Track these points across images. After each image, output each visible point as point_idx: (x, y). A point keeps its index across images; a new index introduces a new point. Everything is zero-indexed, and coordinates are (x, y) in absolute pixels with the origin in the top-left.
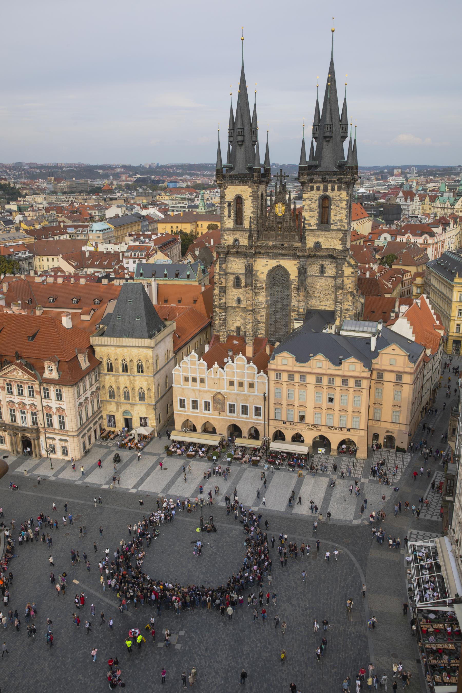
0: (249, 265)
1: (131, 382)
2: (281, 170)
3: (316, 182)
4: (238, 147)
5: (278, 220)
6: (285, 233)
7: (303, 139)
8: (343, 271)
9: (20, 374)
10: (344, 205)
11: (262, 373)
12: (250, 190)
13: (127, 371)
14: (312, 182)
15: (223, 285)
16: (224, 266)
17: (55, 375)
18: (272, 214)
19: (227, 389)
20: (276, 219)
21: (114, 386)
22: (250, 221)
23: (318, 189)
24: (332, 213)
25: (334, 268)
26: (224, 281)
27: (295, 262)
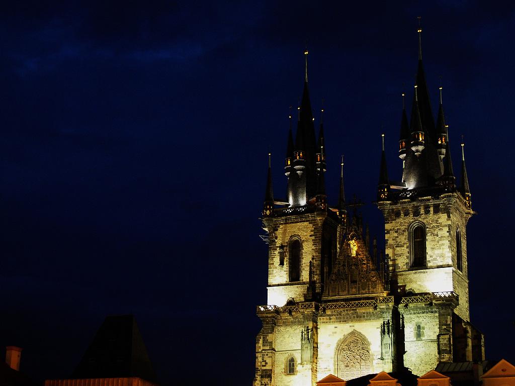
15: (268, 367)
22: (310, 269)
23: (407, 214)
26: (269, 360)
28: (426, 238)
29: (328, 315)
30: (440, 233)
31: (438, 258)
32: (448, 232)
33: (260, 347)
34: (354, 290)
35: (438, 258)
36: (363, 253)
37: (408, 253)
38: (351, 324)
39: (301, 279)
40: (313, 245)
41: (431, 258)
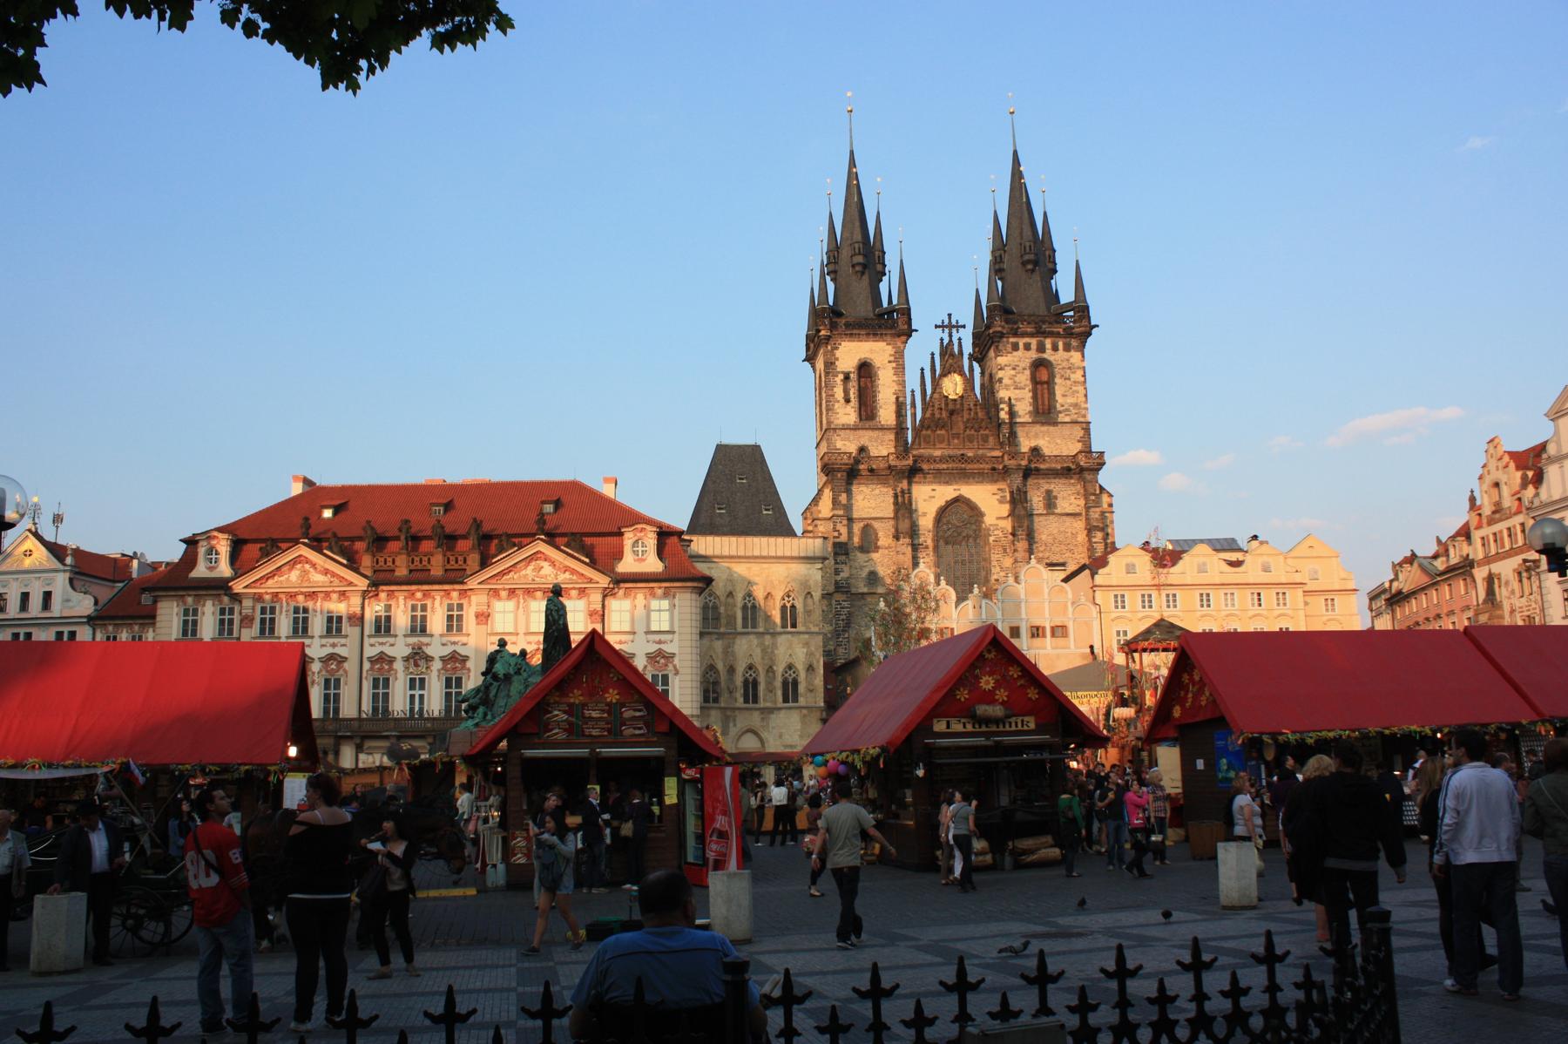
0: (903, 492)
1: (764, 651)
3: (1024, 335)
5: (951, 407)
8: (1098, 496)
9: (547, 569)
10: (1078, 376)
11: (1083, 600)
12: (889, 350)
13: (754, 626)
14: (1016, 335)
15: (844, 538)
16: (843, 498)
17: (653, 564)
21: (720, 666)
23: (1027, 347)
27: (993, 488)
30: (1073, 377)
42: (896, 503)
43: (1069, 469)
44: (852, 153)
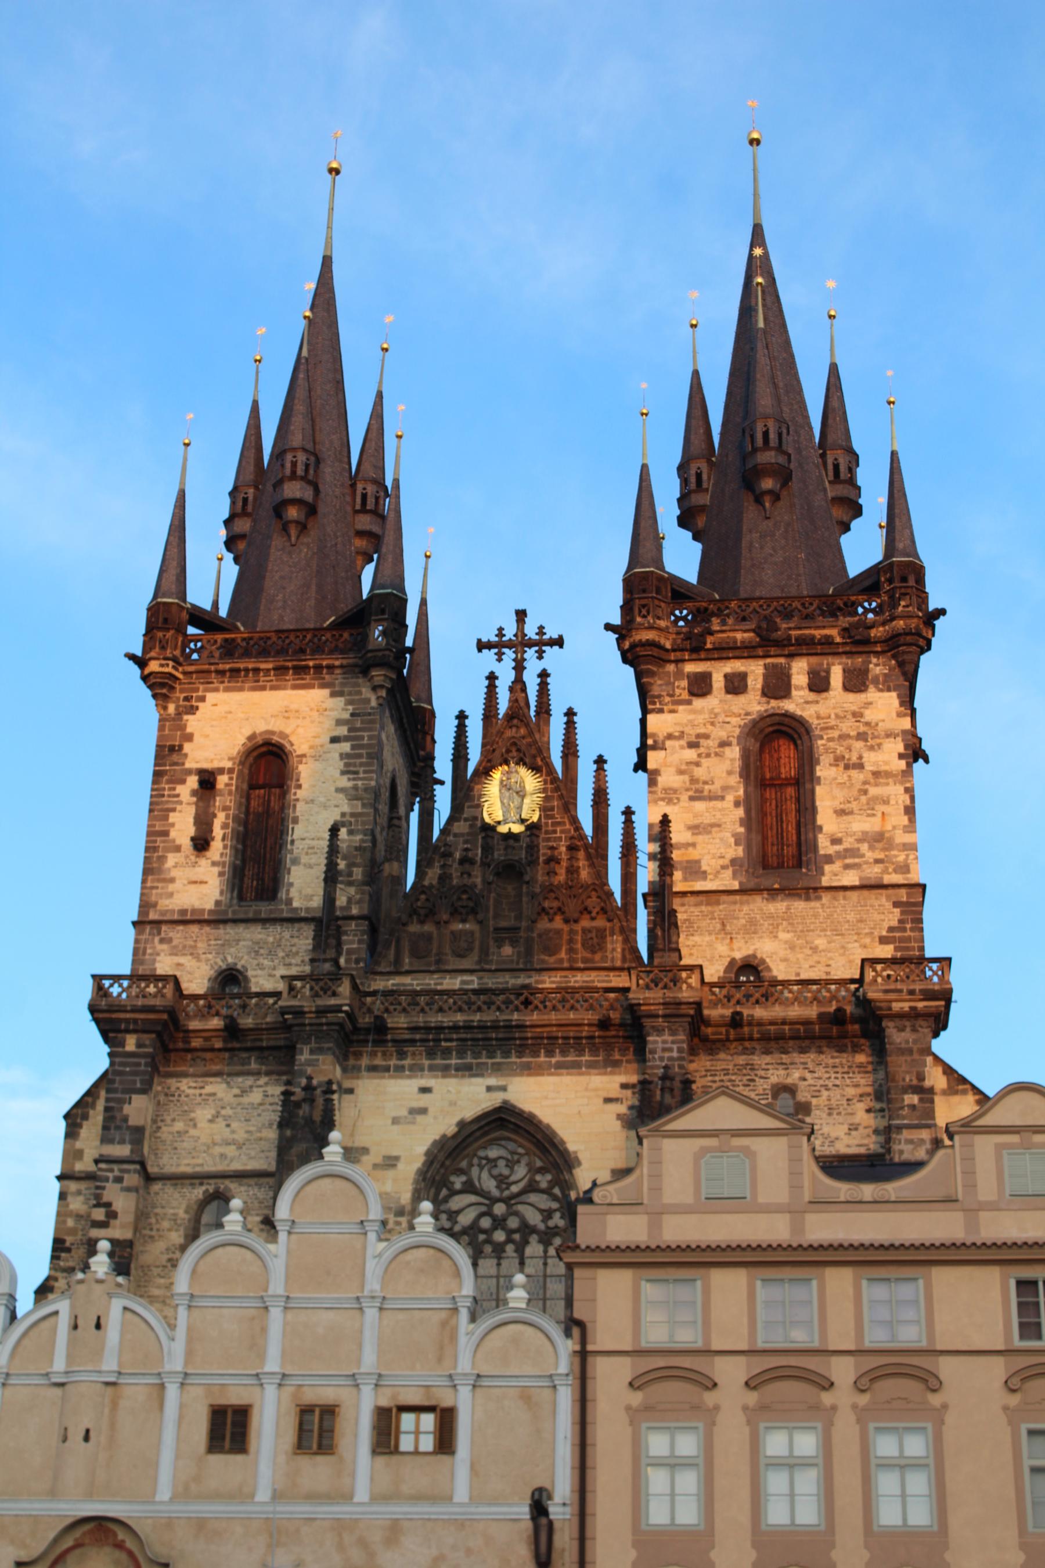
0: (309, 1088)
2: (521, 615)
3: (725, 651)
4: (277, 542)
5: (499, 855)
6: (543, 924)
7: (644, 468)
8: (927, 1094)
11: (518, 1297)
16: (137, 1109)
18: (461, 827)
19: (183, 1493)
20: (487, 849)
22: (333, 850)
23: (736, 685)
24: (826, 800)
25: (860, 1108)
26: (123, 1203)
27: (610, 1082)
28: (812, 771)
29: (394, 1041)
30: (872, 760)
31: (864, 847)
32: (901, 756)
33: (79, 1154)
34: (507, 950)
35: (864, 847)
36: (552, 817)
37: (741, 825)
38: (492, 1081)
39: (282, 895)
40: (343, 773)
41: (838, 848)
42: (281, 1125)
43: (838, 1018)
44: (327, 262)
